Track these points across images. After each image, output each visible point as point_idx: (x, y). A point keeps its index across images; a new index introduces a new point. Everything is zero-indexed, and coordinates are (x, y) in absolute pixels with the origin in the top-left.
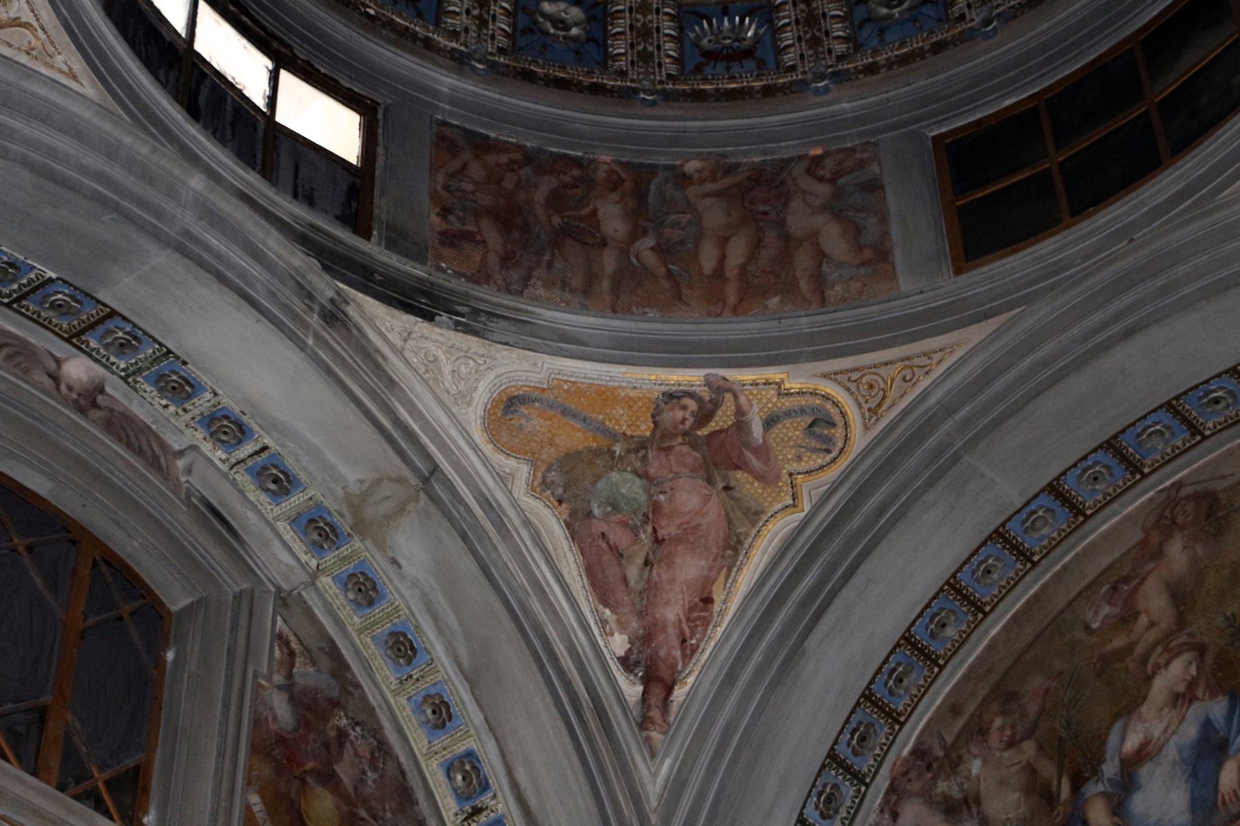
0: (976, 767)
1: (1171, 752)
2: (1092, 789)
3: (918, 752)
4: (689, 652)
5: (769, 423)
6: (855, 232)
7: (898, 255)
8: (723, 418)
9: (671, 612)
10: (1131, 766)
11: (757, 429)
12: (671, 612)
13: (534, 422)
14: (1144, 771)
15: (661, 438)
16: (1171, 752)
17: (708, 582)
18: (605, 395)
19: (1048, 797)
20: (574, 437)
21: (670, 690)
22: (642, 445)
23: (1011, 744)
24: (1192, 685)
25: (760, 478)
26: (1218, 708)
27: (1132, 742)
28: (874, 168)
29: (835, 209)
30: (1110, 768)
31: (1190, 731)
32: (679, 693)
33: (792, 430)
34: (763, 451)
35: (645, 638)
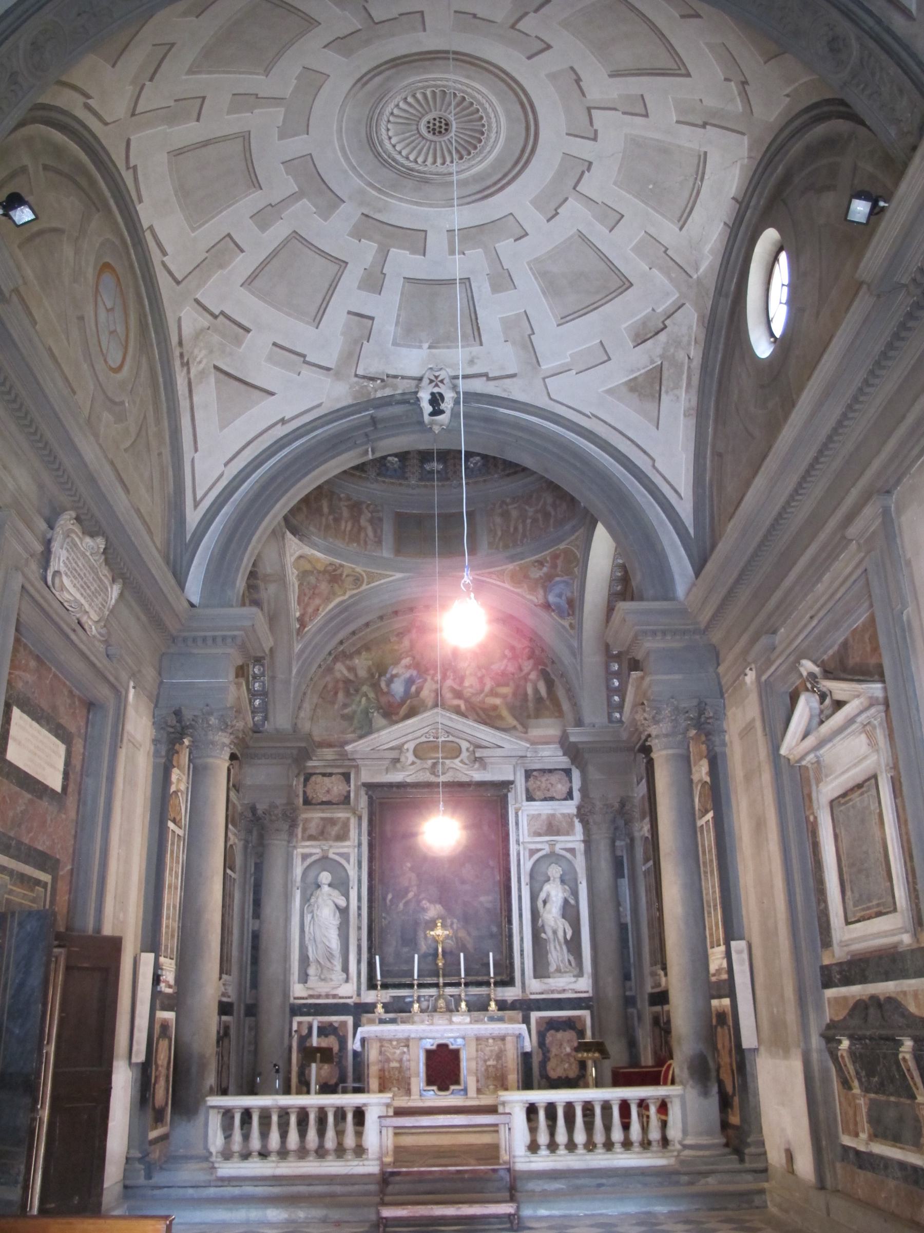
0: (357, 661)
1: (402, 678)
2: (383, 678)
3: (343, 652)
4: (311, 620)
5: (347, 576)
6: (375, 532)
7: (384, 543)
8: (338, 572)
9: (310, 610)
10: (393, 677)
11: (344, 576)
12: (310, 610)
13: (302, 561)
14: (396, 679)
15: (325, 572)
16: (402, 678)
17: (320, 606)
18: (318, 560)
19: (372, 676)
20: (308, 567)
21: (305, 627)
22: (319, 572)
23: (366, 659)
24: (410, 665)
25: (340, 587)
26: (415, 673)
27: (394, 672)
28: (380, 514)
29: (371, 521)
30: (388, 676)
31: (407, 675)
32: (306, 629)
33: (350, 579)
34: (343, 581)
35: (303, 615)
